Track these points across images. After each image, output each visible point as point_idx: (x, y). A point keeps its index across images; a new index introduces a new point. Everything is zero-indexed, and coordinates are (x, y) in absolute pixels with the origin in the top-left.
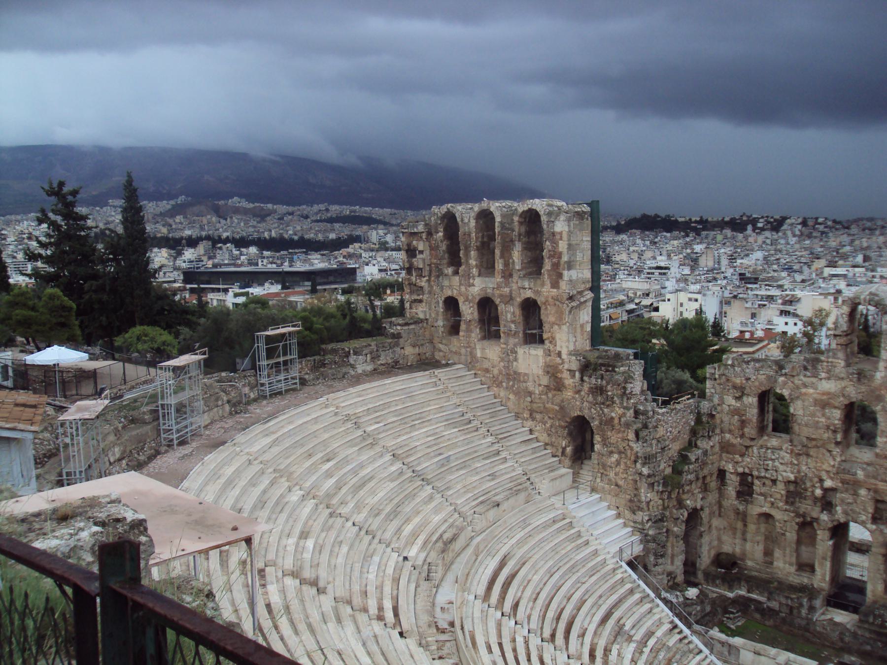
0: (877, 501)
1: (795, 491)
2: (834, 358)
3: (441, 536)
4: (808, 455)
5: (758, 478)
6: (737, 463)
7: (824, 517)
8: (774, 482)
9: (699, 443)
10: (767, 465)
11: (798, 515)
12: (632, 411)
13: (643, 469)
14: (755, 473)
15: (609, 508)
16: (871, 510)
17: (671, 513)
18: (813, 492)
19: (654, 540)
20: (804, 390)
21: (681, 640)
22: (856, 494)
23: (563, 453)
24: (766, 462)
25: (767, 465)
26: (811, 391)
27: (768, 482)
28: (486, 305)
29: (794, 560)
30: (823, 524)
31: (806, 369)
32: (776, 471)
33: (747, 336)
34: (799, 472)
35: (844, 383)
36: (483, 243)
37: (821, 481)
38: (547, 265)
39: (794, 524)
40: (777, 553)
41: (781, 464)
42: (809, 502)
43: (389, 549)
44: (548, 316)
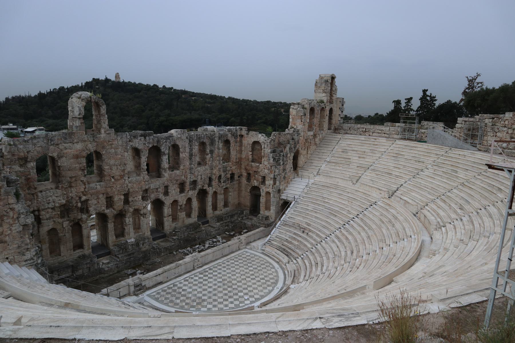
1: (65, 210)
2: (80, 130)
4: (71, 187)
5: (43, 210)
8: (52, 209)
10: (49, 200)
11: (71, 221)
13: (27, 220)
20: (65, 151)
22: (98, 198)
24: (48, 199)
25: (49, 200)
26: (70, 151)
27: (50, 210)
31: (66, 139)
32: (54, 202)
34: (68, 197)
35: (87, 143)
37: (80, 198)
39: (69, 227)
41: (57, 197)
42: (75, 212)
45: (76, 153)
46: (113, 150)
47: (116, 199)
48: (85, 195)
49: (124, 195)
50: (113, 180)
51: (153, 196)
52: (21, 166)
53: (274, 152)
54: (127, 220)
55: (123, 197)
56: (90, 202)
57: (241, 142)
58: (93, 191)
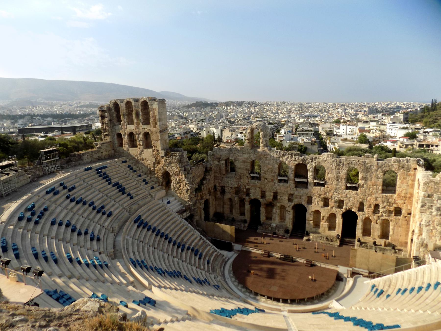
0: (262, 191)
1: (238, 191)
3: (118, 217)
6: (220, 183)
7: (247, 198)
8: (231, 188)
9: (207, 177)
11: (239, 198)
12: (183, 168)
14: (225, 186)
15: (178, 202)
16: (260, 194)
17: (199, 201)
18: (243, 190)
19: (194, 210)
21: (203, 242)
22: (256, 190)
23: (162, 185)
27: (230, 188)
28: (131, 135)
29: (239, 213)
30: (246, 200)
33: (229, 141)
35: (250, 155)
36: (129, 113)
37: (245, 186)
38: (151, 120)
40: (234, 211)
42: (242, 193)
43: (97, 224)
44: (153, 137)
45: (244, 160)
46: (267, 162)
47: (267, 194)
48: (248, 185)
49: (274, 193)
50: (266, 181)
51: (296, 201)
52: (219, 162)
53: (430, 196)
54: (274, 210)
55: (272, 194)
56: (251, 190)
57: (415, 175)
58: (253, 184)
